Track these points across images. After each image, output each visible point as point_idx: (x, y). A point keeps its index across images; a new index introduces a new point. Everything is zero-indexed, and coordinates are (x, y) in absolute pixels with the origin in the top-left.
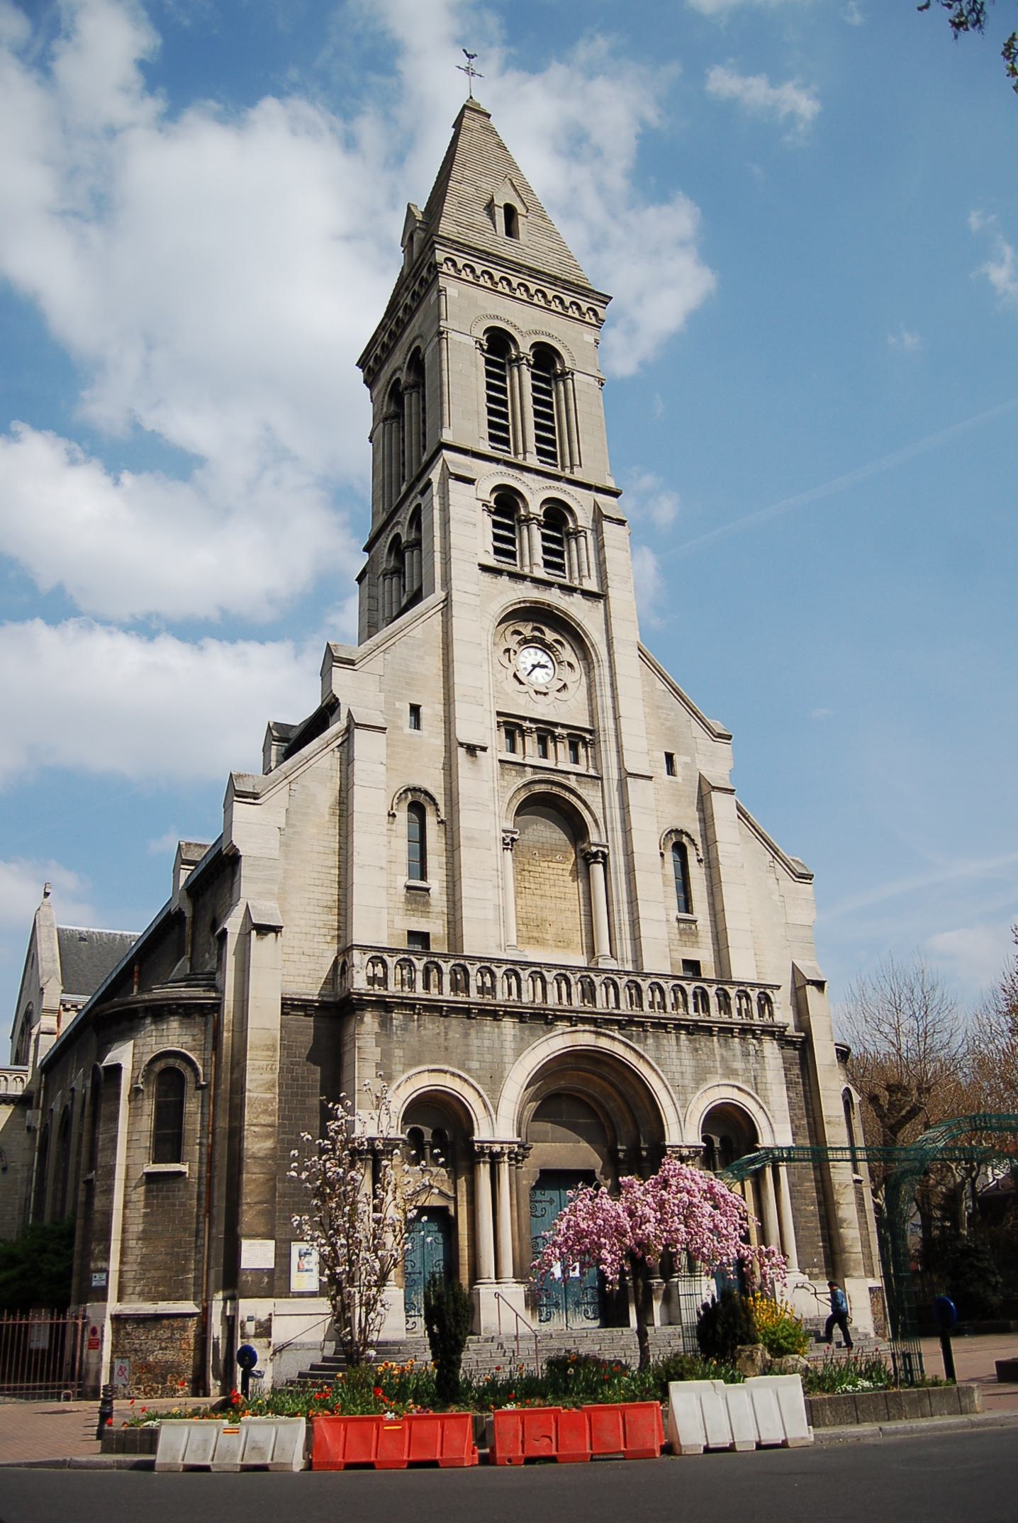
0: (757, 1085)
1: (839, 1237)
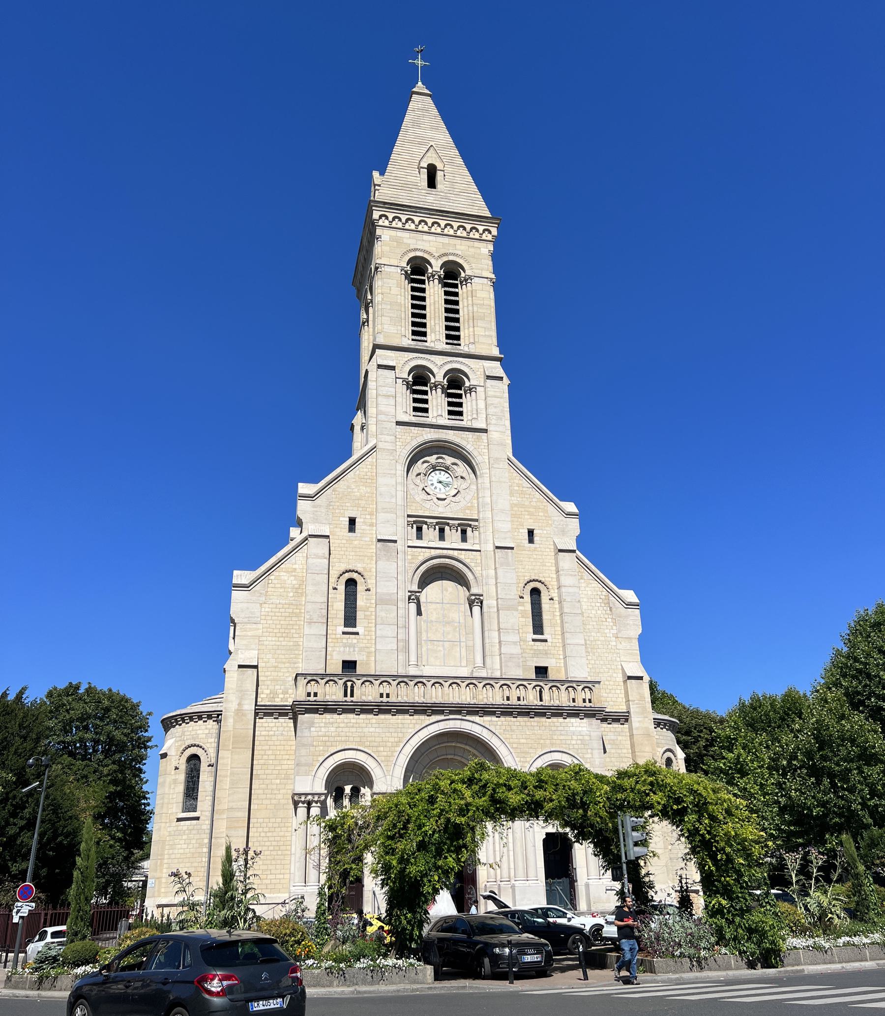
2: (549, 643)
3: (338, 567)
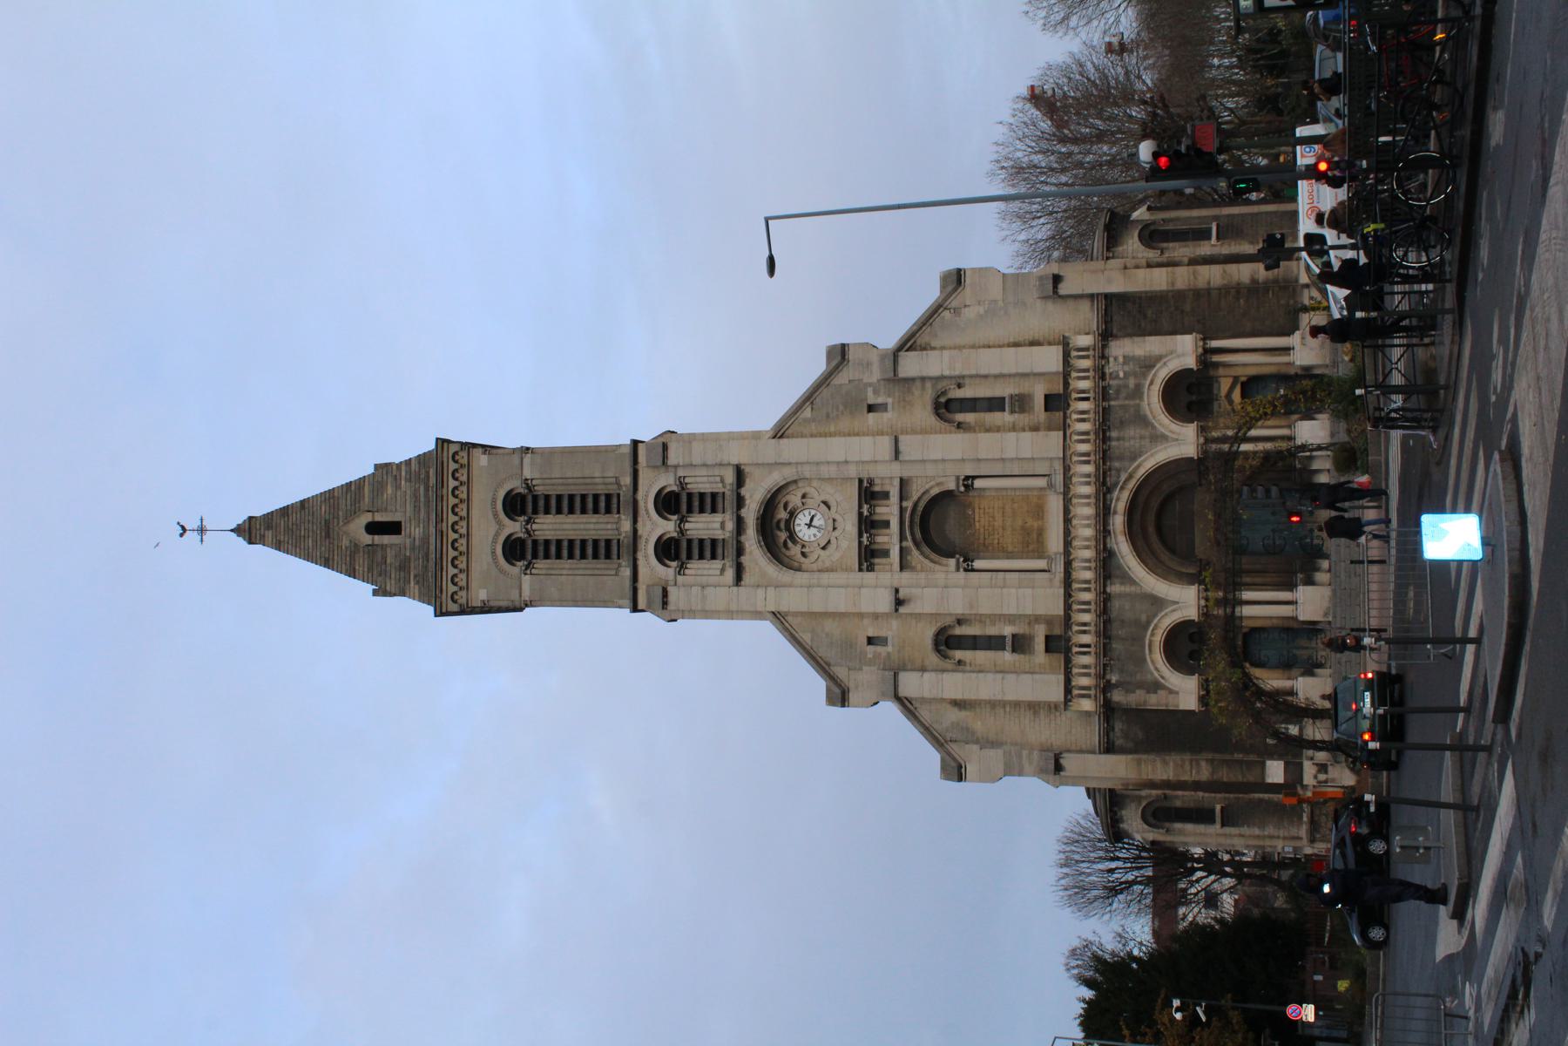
0: (1148, 364)
1: (1266, 282)
3: (933, 659)
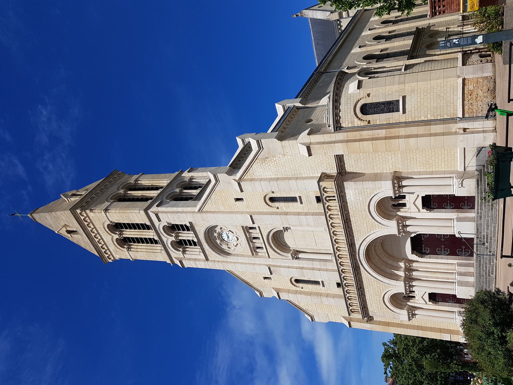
2: (301, 195)
